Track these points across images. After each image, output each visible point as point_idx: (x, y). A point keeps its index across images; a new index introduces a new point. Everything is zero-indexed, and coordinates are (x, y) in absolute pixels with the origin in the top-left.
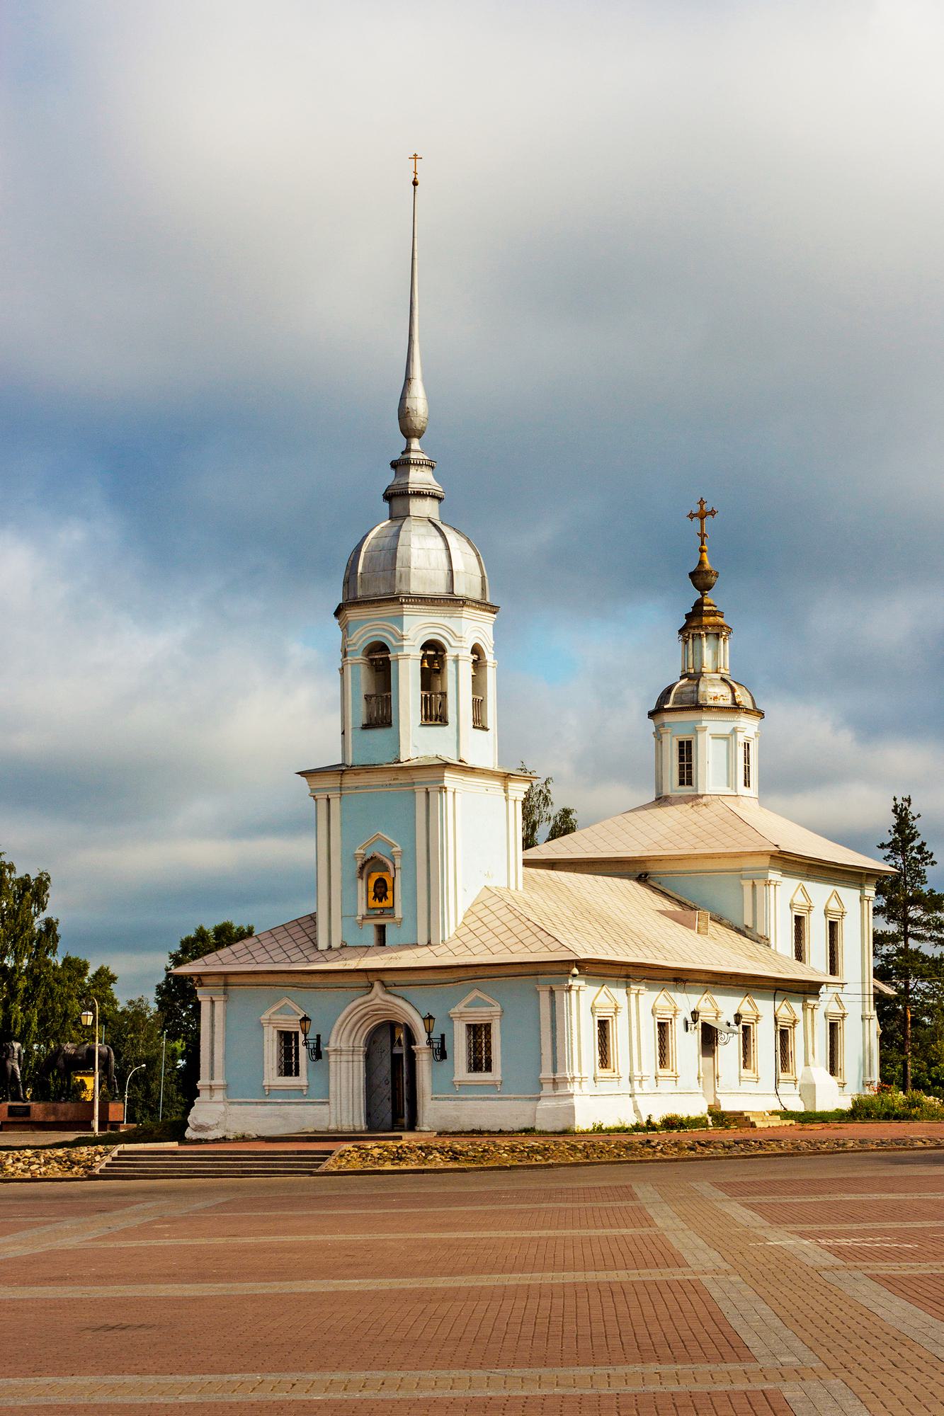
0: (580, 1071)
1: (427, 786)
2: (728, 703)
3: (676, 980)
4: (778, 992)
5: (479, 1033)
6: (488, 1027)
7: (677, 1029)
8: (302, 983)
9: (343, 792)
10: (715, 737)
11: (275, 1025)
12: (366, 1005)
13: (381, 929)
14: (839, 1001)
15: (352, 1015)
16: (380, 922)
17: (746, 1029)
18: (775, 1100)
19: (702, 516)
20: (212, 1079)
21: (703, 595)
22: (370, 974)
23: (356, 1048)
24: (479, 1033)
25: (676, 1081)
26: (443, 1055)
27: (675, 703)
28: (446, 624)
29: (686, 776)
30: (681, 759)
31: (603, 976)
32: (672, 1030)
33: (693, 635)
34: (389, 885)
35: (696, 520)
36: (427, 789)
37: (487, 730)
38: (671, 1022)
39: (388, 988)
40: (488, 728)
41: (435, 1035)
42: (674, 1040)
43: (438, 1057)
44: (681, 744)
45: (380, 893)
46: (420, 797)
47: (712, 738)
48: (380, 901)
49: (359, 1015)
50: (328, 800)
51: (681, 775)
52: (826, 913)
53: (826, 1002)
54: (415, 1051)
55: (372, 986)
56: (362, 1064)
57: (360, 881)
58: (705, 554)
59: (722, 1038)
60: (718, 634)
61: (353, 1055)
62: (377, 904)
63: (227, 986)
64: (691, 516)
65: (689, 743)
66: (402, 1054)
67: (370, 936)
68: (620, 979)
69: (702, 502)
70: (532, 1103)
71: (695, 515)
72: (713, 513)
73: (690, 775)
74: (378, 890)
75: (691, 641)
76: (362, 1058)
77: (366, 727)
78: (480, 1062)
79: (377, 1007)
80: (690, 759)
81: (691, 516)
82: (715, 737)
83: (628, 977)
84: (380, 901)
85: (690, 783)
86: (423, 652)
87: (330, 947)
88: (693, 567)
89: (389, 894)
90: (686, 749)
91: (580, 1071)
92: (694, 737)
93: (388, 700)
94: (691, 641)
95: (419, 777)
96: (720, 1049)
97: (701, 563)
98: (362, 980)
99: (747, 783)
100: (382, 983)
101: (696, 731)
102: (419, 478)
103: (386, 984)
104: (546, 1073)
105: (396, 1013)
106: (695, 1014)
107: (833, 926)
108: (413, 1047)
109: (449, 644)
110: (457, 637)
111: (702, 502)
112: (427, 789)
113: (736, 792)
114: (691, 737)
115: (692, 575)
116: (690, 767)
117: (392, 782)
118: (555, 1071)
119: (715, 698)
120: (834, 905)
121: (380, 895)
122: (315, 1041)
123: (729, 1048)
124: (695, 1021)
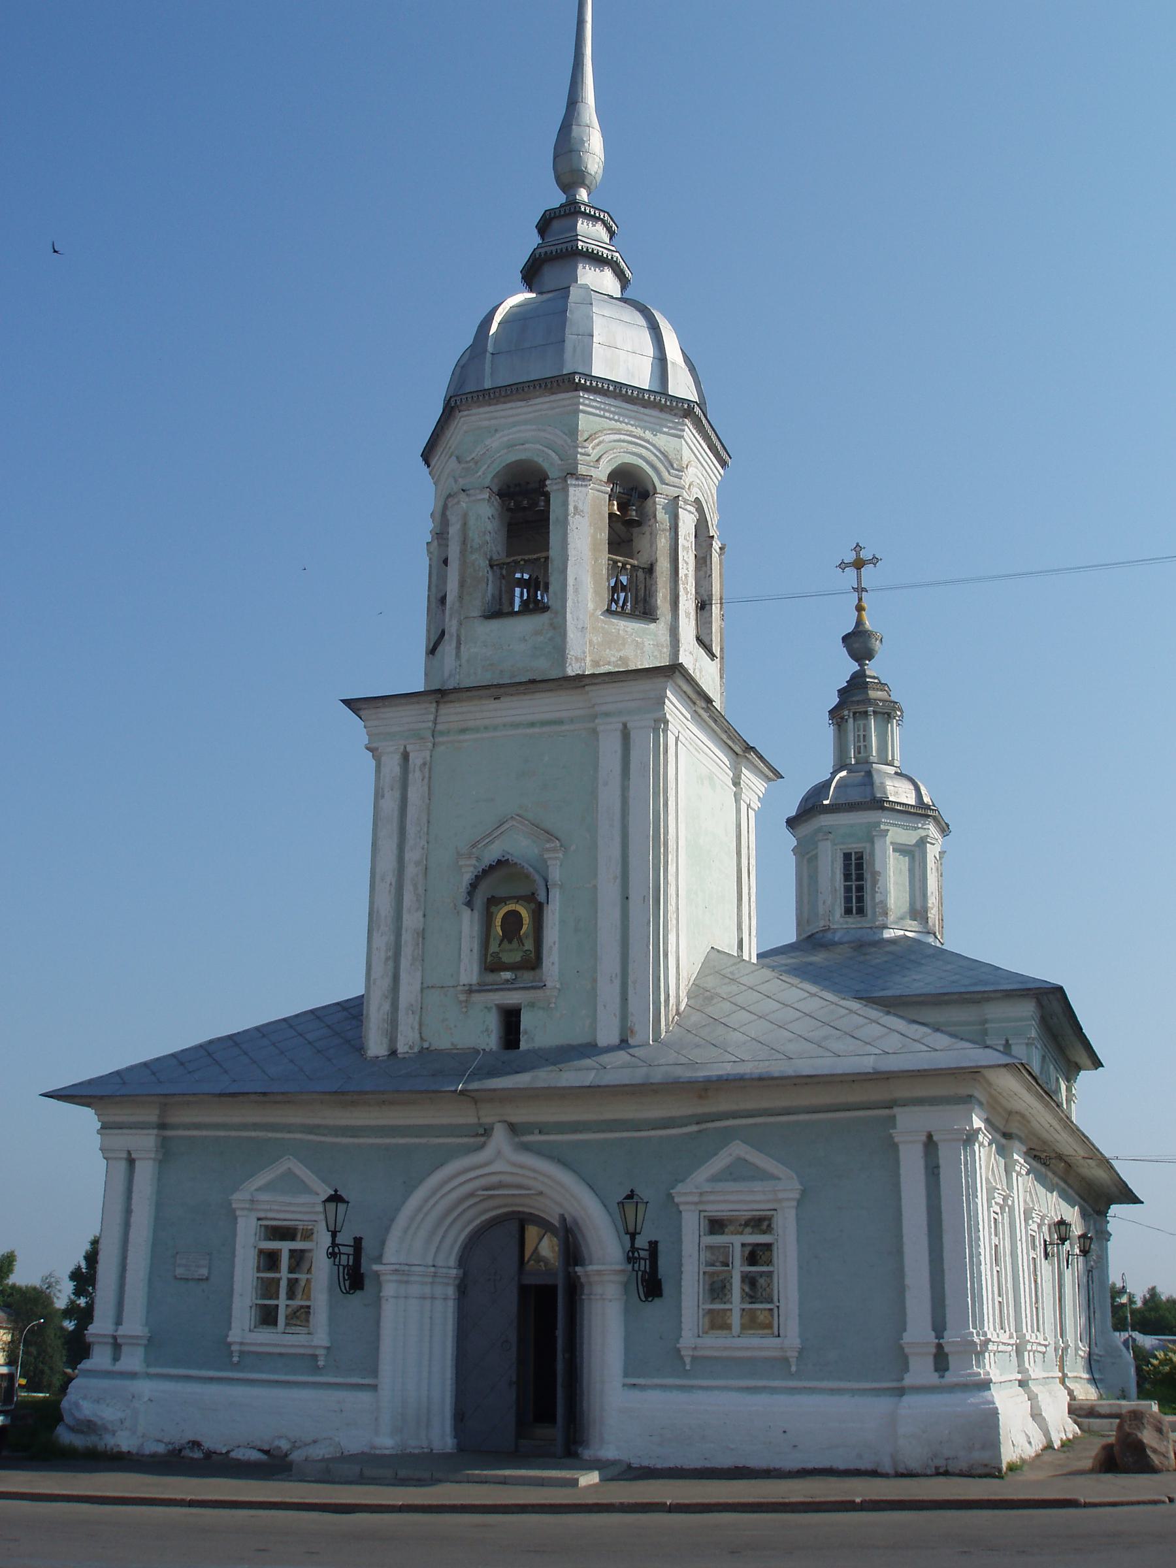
1: (624, 719)
11: (262, 1215)
13: (511, 1020)
15: (438, 1196)
16: (512, 998)
19: (859, 564)
20: (119, 1322)
21: (862, 665)
23: (441, 1270)
30: (847, 877)
33: (854, 713)
35: (851, 572)
36: (625, 726)
41: (642, 1242)
44: (847, 856)
46: (610, 745)
49: (454, 1196)
51: (848, 900)
54: (583, 1280)
55: (487, 1132)
56: (451, 1304)
57: (466, 913)
61: (432, 1283)
64: (843, 566)
65: (860, 857)
66: (554, 1288)
69: (858, 548)
70: (883, 1404)
72: (874, 561)
73: (860, 899)
76: (451, 1291)
79: (494, 1179)
80: (860, 877)
81: (843, 566)
85: (861, 911)
87: (393, 1053)
88: (850, 628)
92: (868, 845)
95: (606, 697)
100: (514, 1129)
102: (590, 233)
105: (541, 1193)
108: (578, 1269)
111: (858, 548)
112: (625, 726)
114: (863, 845)
115: (846, 639)
116: (860, 889)
122: (350, 1250)
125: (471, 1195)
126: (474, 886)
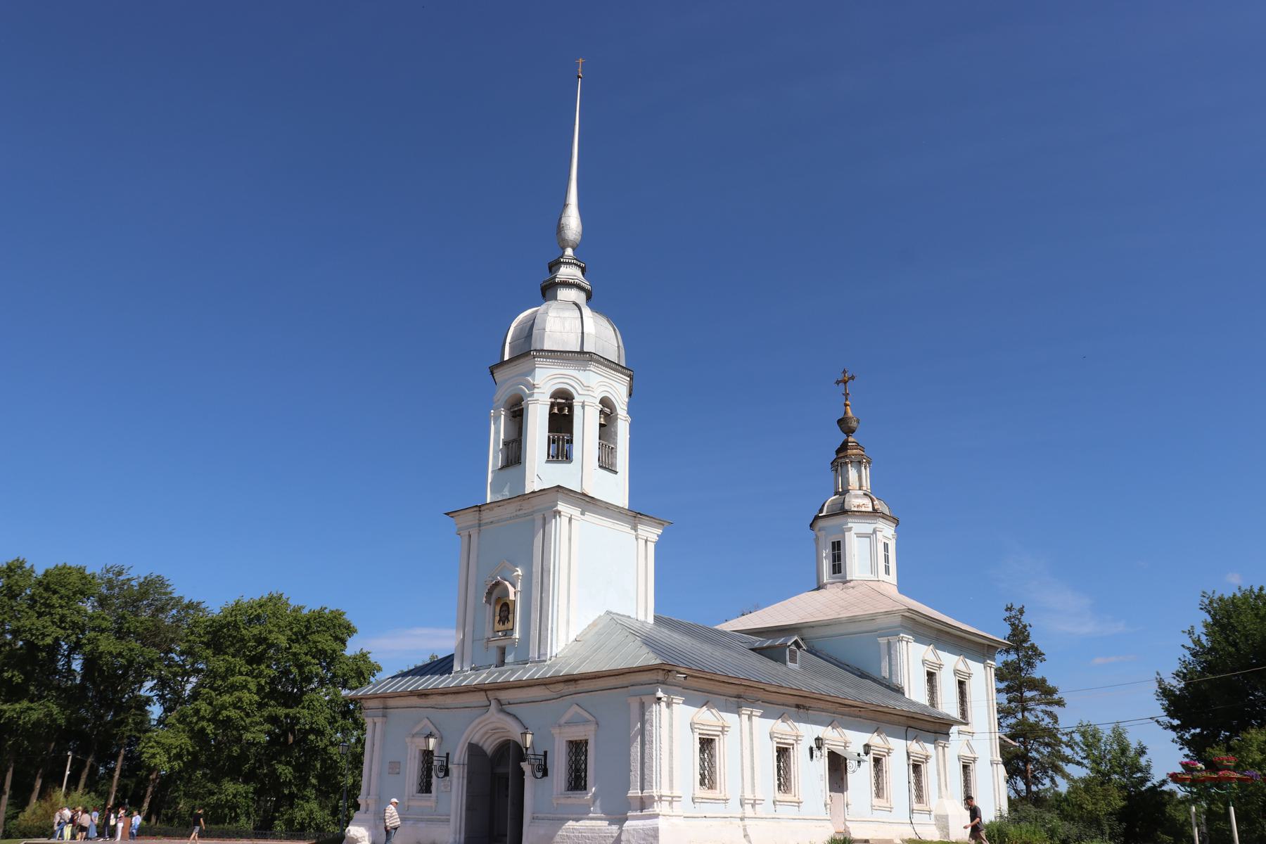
0: (671, 787)
2: (870, 509)
3: (798, 706)
4: (909, 729)
5: (578, 749)
6: (586, 742)
7: (799, 756)
8: (439, 705)
9: (481, 528)
10: (859, 535)
12: (484, 724)
14: (969, 746)
16: (501, 643)
17: (877, 761)
18: (910, 828)
22: (489, 693)
24: (578, 749)
25: (799, 807)
26: (545, 773)
27: (827, 512)
28: (575, 375)
29: (837, 567)
31: (708, 693)
32: (794, 756)
34: (511, 608)
37: (616, 472)
38: (793, 748)
39: (504, 707)
40: (617, 471)
42: (796, 765)
43: (539, 774)
44: (833, 543)
45: (504, 616)
47: (857, 537)
48: (504, 624)
50: (470, 536)
52: (956, 672)
53: (957, 743)
57: (488, 605)
58: (848, 407)
59: (851, 764)
60: (859, 462)
62: (501, 627)
63: (386, 708)
64: (838, 382)
66: (508, 773)
67: (494, 657)
68: (730, 699)
71: (840, 382)
74: (502, 614)
75: (839, 468)
77: (502, 468)
78: (577, 781)
81: (838, 382)
82: (859, 535)
83: (739, 697)
84: (504, 624)
86: (553, 400)
89: (510, 617)
90: (837, 547)
91: (671, 787)
93: (521, 440)
94: (839, 468)
96: (852, 778)
97: (846, 413)
98: (479, 699)
99: (887, 571)
101: (843, 532)
103: (503, 702)
104: (634, 792)
106: (819, 741)
107: (961, 684)
109: (577, 391)
110: (585, 386)
112: (544, 515)
113: (878, 577)
117: (518, 513)
118: (642, 789)
119: (858, 506)
120: (961, 667)
121: (504, 619)
123: (860, 776)
124: (819, 748)
125: (486, 733)
126: (490, 593)
